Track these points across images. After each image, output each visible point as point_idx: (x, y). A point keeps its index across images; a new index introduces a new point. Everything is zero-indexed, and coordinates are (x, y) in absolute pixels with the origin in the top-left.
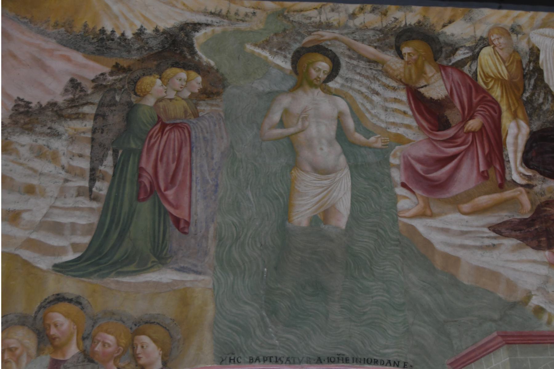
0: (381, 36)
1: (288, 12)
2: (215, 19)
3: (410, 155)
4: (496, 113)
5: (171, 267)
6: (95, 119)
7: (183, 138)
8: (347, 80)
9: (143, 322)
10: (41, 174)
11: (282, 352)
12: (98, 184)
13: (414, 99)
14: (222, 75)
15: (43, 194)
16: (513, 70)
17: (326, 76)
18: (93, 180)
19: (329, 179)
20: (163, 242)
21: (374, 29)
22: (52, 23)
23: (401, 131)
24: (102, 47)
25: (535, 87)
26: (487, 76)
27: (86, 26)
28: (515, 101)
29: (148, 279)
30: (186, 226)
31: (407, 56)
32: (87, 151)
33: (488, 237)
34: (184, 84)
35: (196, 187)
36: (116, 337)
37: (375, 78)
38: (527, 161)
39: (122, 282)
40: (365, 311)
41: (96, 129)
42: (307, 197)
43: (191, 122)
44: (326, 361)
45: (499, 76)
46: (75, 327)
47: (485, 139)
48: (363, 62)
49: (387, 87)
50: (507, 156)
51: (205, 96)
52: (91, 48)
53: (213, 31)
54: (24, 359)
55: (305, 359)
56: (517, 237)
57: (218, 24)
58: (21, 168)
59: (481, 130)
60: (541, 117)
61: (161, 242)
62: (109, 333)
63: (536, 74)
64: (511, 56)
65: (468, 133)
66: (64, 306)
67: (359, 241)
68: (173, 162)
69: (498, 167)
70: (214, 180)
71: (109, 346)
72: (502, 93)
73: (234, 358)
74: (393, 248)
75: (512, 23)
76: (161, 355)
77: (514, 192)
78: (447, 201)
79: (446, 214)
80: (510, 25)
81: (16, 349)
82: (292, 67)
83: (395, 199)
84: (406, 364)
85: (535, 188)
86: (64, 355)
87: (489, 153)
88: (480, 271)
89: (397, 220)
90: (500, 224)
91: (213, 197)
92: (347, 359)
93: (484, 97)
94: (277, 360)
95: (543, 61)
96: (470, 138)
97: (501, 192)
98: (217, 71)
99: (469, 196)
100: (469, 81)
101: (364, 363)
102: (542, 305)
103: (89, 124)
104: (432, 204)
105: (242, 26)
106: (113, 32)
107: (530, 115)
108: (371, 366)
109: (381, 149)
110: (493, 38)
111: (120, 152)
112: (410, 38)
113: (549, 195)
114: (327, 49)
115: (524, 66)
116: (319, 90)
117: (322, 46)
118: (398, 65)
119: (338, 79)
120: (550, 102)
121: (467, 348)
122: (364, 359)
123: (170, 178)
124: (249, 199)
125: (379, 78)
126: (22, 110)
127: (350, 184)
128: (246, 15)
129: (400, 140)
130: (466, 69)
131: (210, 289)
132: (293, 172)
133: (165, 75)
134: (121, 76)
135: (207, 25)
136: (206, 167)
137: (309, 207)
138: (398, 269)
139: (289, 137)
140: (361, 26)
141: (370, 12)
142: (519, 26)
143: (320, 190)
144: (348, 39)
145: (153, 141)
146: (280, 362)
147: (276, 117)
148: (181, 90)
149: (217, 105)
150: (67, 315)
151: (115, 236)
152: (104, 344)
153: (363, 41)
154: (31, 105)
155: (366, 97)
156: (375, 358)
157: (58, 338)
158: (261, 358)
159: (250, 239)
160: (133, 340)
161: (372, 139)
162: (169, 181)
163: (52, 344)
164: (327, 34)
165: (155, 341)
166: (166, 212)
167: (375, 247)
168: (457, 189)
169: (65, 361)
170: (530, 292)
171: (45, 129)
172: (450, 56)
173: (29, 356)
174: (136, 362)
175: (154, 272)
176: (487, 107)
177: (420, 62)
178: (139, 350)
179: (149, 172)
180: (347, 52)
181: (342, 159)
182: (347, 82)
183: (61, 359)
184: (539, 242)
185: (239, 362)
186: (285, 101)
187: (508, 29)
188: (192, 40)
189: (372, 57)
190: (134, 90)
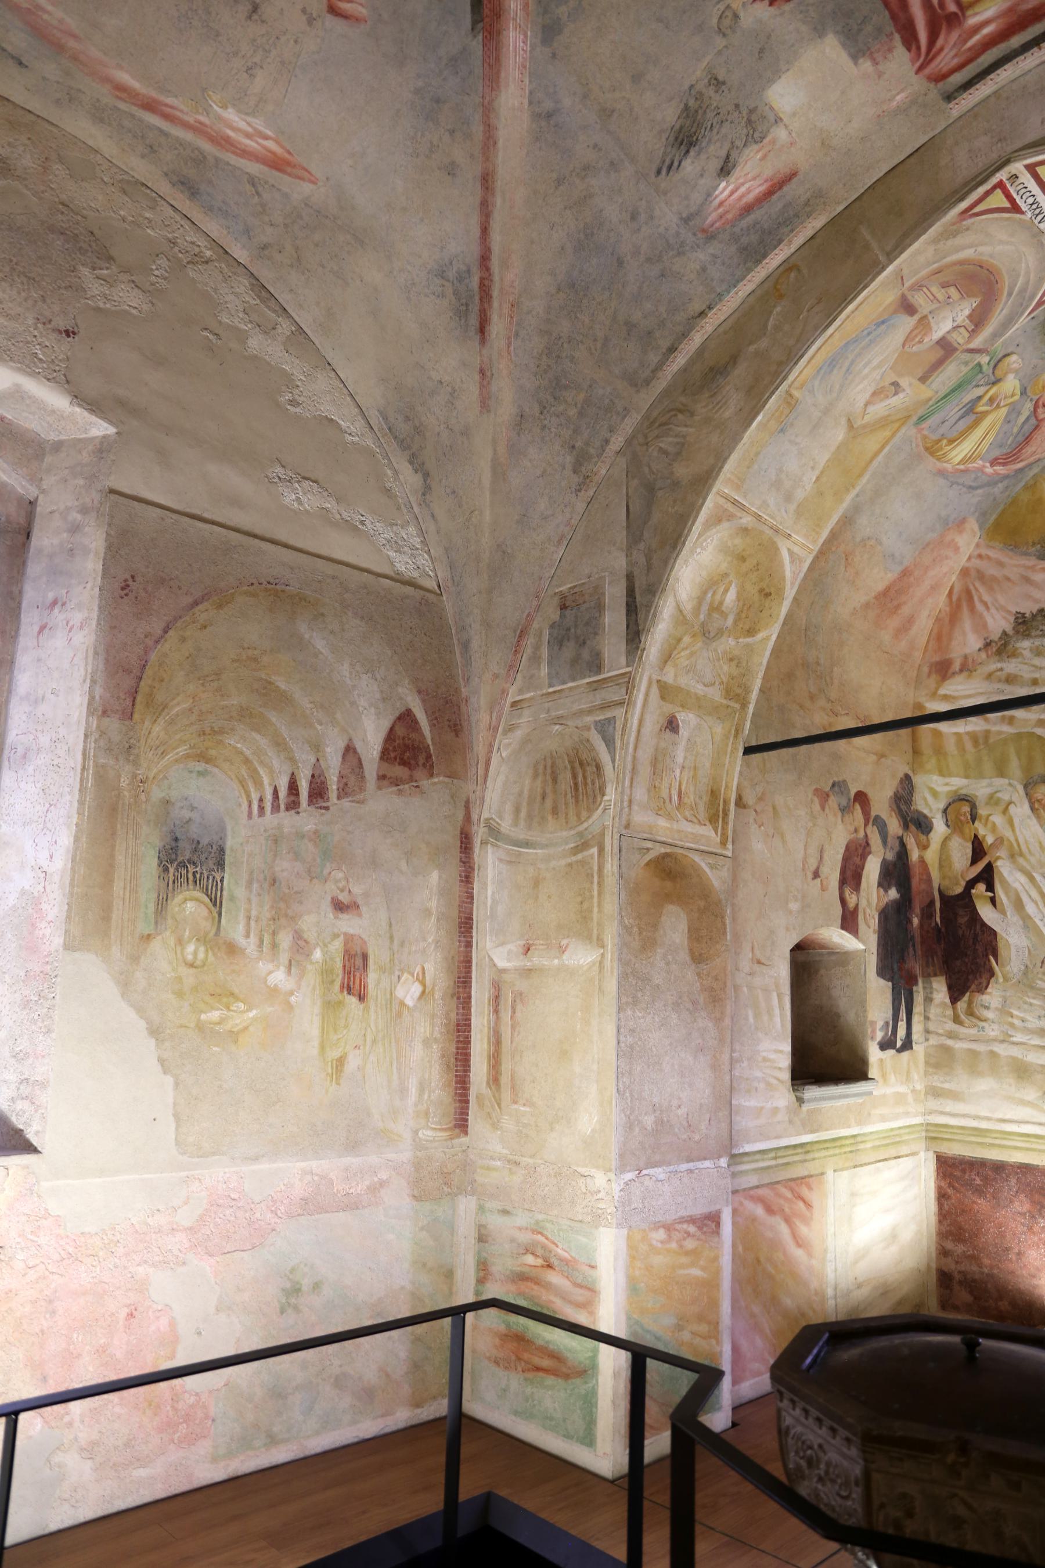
10: (1041, 668)
22: (1030, 541)
126: (1020, 621)
171: (1039, 633)
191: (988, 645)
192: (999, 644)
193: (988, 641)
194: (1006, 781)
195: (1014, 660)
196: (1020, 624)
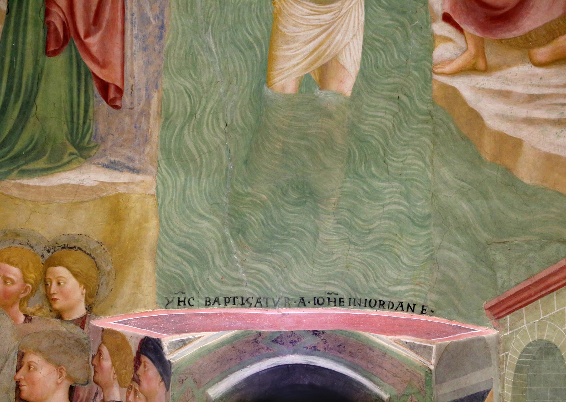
5: (96, 162)
9: (58, 247)
11: (251, 291)
19: (331, 11)
20: (84, 123)
29: (65, 181)
30: (119, 96)
35: (132, 30)
36: (22, 270)
39: (28, 186)
40: (371, 227)
42: (297, 45)
44: (312, 302)
55: (282, 300)
62: (12, 264)
67: (370, 116)
70: (158, 18)
71: (13, 282)
73: (185, 299)
74: (420, 126)
76: (84, 296)
78: (513, 44)
79: (509, 66)
84: (425, 308)
89: (431, 79)
91: (157, 47)
92: (342, 300)
94: (244, 302)
101: (365, 306)
104: (488, 50)
108: (375, 310)
121: (518, 284)
122: (366, 300)
123: (92, 15)
124: (210, 50)
127: (362, 19)
131: (152, 195)
137: (298, 62)
138: (424, 161)
143: (318, 30)
146: (247, 304)
151: (16, 113)
158: (221, 299)
159: (211, 115)
160: (45, 274)
162: (91, 20)
167: (394, 126)
174: (51, 306)
175: (72, 169)
178: (54, 288)
179: (60, 5)
185: (191, 304)
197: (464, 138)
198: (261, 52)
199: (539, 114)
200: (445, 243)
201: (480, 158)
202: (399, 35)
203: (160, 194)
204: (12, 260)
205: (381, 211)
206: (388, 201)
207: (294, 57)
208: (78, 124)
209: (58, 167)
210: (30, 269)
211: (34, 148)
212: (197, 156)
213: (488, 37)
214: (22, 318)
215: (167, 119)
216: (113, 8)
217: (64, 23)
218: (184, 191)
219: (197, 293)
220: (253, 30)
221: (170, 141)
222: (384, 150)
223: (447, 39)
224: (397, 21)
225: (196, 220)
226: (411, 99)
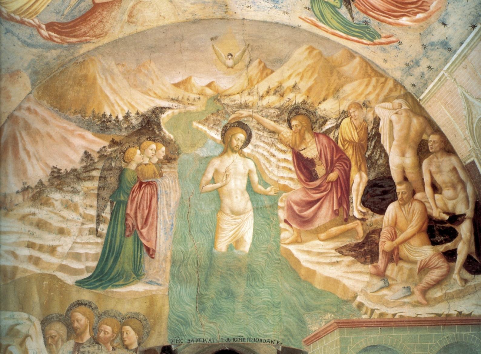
0: (279, 112)
1: (221, 97)
2: (175, 104)
3: (291, 200)
4: (347, 167)
6: (99, 180)
7: (153, 191)
8: (255, 146)
10: (67, 220)
12: (102, 226)
13: (296, 158)
14: (178, 145)
15: (69, 234)
16: (362, 135)
17: (242, 144)
18: (99, 222)
20: (139, 264)
21: (274, 108)
23: (287, 183)
24: (104, 127)
25: (375, 147)
26: (344, 140)
27: (93, 112)
28: (361, 158)
29: (130, 290)
31: (294, 127)
32: (95, 203)
33: (334, 256)
34: (154, 152)
37: (273, 145)
38: (364, 203)
39: (116, 292)
41: (100, 187)
43: (158, 181)
45: (352, 140)
46: (88, 322)
47: (339, 187)
48: (266, 133)
49: (280, 150)
50: (352, 198)
51: (167, 161)
52: (97, 128)
53: (173, 113)
54: (60, 343)
56: (352, 256)
57: (176, 108)
58: (56, 216)
59: (337, 180)
60: (376, 169)
61: (138, 264)
62: (108, 325)
63: (376, 137)
64: (361, 124)
65: (329, 182)
66: (83, 308)
68: (146, 210)
69: (345, 207)
71: (108, 333)
72: (353, 152)
74: (277, 265)
75: (364, 99)
77: (354, 224)
80: (363, 101)
81: (55, 336)
82: (222, 138)
83: (279, 231)
85: (367, 221)
86: (82, 340)
87: (341, 197)
88: (328, 279)
89: (280, 246)
90: (343, 247)
93: (341, 156)
95: (381, 128)
96: (330, 186)
97: (346, 224)
98: (175, 142)
99: (325, 228)
100: (332, 144)
102: (363, 302)
103: (96, 184)
104: (302, 234)
105: (191, 108)
106: (111, 115)
107: (369, 168)
109: (273, 196)
110: (351, 111)
111: (115, 203)
112: (297, 114)
113: (375, 226)
114: (244, 124)
115: (369, 132)
116: (237, 154)
117: (241, 122)
118: (288, 134)
119: (250, 146)
120: (383, 158)
123: (144, 220)
125: (276, 144)
126: (56, 175)
127: (253, 221)
128: (194, 100)
129: (285, 189)
130: (331, 136)
131: (167, 295)
132: (218, 214)
133: (142, 146)
134: (115, 149)
135: (169, 108)
136: (166, 213)
138: (278, 280)
139: (217, 189)
140: (266, 106)
141: (273, 95)
142: (369, 101)
143: (234, 226)
144: (258, 116)
145: (134, 194)
147: (210, 176)
148: (152, 157)
149: (174, 168)
150: (84, 314)
152: (105, 332)
153: (267, 117)
154: (60, 171)
155: (267, 159)
156: (261, 338)
157: (79, 329)
158: (194, 339)
160: (121, 329)
161: (269, 189)
163: (75, 333)
164: (245, 112)
165: (134, 329)
166: (142, 244)
168: (319, 222)
169: (83, 343)
170: (357, 293)
171: (70, 189)
172: (322, 126)
173: (63, 341)
175: (133, 285)
176: (342, 163)
177: (302, 131)
178: (125, 335)
180: (257, 126)
181: (250, 204)
182: (255, 148)
183: (81, 342)
184: (366, 259)
186: (216, 163)
187: (361, 104)
188: (159, 120)
189: (272, 129)
190: (123, 158)
191: (26, 189)
192: (36, 191)
193: (26, 186)
194: (25, 315)
195: (46, 208)
196: (55, 177)
197: (293, 270)
198: (212, 235)
199: (322, 260)
200: (287, 314)
201: (300, 278)
202: (267, 228)
203: (170, 295)
204: (108, 323)
205: (261, 301)
206: (264, 296)
207: (225, 236)
208: (137, 265)
209: (128, 284)
210: (115, 327)
211: (119, 275)
212: (185, 277)
213: (302, 229)
214: (111, 348)
215: (173, 262)
216: (153, 218)
217: (133, 224)
218: (180, 293)
219: (184, 337)
220: (209, 225)
221: (174, 272)
222: (262, 275)
223: (286, 230)
224: (266, 222)
225: (184, 306)
226: (272, 254)
